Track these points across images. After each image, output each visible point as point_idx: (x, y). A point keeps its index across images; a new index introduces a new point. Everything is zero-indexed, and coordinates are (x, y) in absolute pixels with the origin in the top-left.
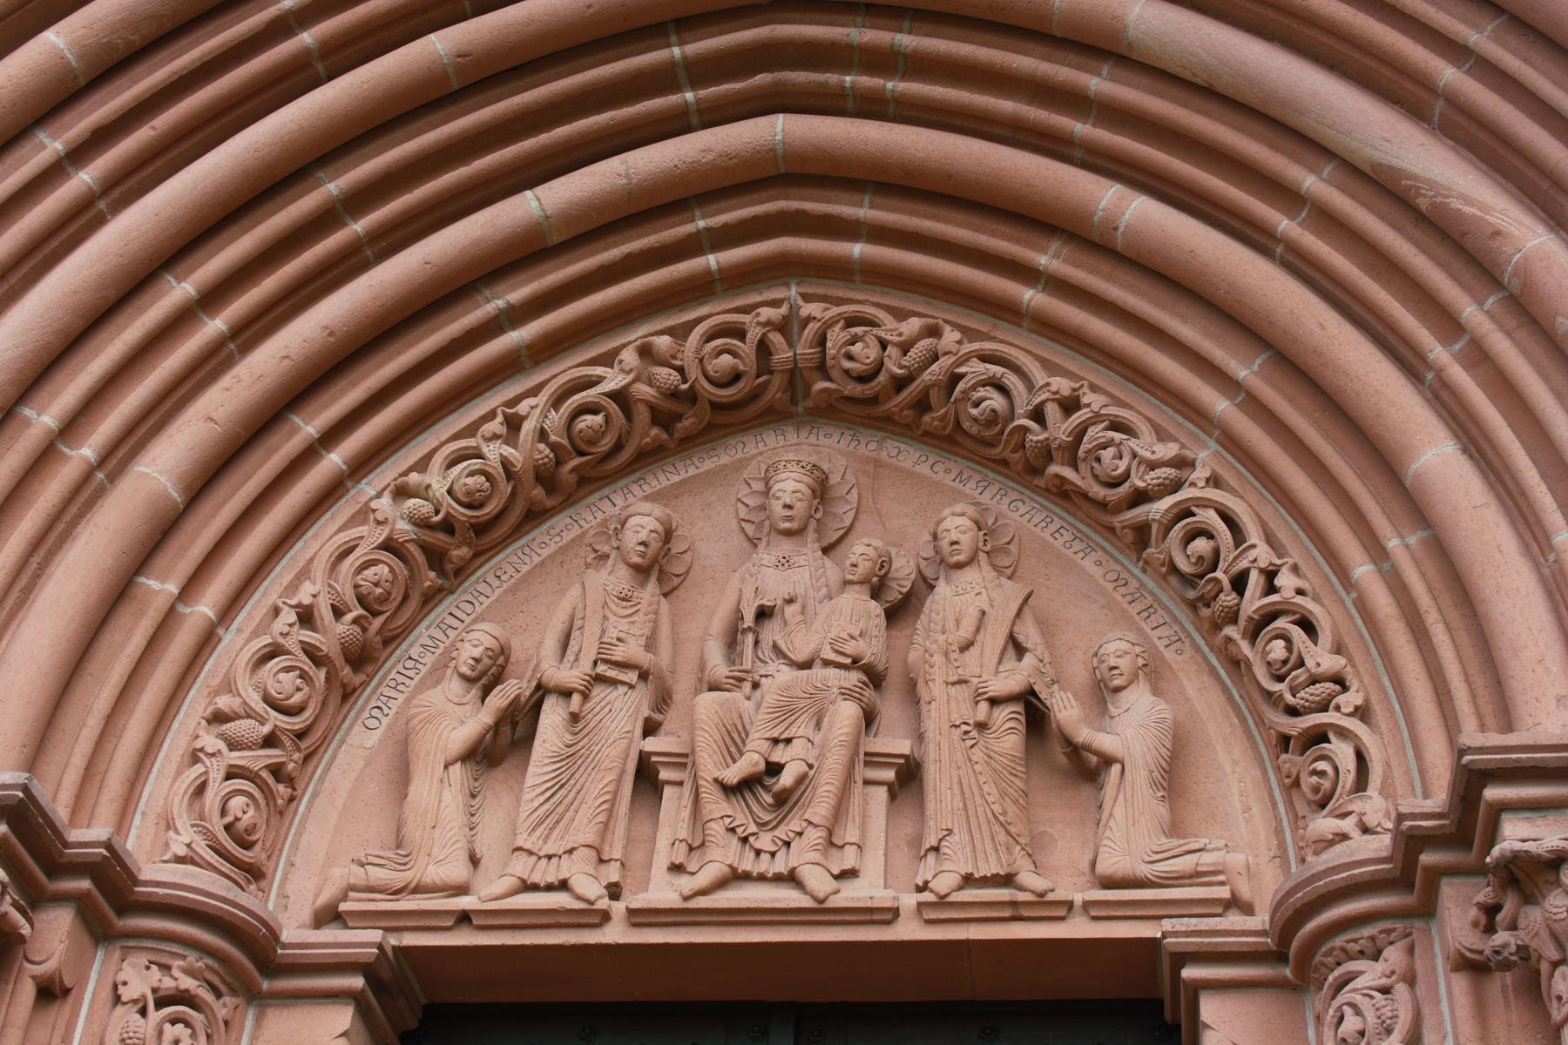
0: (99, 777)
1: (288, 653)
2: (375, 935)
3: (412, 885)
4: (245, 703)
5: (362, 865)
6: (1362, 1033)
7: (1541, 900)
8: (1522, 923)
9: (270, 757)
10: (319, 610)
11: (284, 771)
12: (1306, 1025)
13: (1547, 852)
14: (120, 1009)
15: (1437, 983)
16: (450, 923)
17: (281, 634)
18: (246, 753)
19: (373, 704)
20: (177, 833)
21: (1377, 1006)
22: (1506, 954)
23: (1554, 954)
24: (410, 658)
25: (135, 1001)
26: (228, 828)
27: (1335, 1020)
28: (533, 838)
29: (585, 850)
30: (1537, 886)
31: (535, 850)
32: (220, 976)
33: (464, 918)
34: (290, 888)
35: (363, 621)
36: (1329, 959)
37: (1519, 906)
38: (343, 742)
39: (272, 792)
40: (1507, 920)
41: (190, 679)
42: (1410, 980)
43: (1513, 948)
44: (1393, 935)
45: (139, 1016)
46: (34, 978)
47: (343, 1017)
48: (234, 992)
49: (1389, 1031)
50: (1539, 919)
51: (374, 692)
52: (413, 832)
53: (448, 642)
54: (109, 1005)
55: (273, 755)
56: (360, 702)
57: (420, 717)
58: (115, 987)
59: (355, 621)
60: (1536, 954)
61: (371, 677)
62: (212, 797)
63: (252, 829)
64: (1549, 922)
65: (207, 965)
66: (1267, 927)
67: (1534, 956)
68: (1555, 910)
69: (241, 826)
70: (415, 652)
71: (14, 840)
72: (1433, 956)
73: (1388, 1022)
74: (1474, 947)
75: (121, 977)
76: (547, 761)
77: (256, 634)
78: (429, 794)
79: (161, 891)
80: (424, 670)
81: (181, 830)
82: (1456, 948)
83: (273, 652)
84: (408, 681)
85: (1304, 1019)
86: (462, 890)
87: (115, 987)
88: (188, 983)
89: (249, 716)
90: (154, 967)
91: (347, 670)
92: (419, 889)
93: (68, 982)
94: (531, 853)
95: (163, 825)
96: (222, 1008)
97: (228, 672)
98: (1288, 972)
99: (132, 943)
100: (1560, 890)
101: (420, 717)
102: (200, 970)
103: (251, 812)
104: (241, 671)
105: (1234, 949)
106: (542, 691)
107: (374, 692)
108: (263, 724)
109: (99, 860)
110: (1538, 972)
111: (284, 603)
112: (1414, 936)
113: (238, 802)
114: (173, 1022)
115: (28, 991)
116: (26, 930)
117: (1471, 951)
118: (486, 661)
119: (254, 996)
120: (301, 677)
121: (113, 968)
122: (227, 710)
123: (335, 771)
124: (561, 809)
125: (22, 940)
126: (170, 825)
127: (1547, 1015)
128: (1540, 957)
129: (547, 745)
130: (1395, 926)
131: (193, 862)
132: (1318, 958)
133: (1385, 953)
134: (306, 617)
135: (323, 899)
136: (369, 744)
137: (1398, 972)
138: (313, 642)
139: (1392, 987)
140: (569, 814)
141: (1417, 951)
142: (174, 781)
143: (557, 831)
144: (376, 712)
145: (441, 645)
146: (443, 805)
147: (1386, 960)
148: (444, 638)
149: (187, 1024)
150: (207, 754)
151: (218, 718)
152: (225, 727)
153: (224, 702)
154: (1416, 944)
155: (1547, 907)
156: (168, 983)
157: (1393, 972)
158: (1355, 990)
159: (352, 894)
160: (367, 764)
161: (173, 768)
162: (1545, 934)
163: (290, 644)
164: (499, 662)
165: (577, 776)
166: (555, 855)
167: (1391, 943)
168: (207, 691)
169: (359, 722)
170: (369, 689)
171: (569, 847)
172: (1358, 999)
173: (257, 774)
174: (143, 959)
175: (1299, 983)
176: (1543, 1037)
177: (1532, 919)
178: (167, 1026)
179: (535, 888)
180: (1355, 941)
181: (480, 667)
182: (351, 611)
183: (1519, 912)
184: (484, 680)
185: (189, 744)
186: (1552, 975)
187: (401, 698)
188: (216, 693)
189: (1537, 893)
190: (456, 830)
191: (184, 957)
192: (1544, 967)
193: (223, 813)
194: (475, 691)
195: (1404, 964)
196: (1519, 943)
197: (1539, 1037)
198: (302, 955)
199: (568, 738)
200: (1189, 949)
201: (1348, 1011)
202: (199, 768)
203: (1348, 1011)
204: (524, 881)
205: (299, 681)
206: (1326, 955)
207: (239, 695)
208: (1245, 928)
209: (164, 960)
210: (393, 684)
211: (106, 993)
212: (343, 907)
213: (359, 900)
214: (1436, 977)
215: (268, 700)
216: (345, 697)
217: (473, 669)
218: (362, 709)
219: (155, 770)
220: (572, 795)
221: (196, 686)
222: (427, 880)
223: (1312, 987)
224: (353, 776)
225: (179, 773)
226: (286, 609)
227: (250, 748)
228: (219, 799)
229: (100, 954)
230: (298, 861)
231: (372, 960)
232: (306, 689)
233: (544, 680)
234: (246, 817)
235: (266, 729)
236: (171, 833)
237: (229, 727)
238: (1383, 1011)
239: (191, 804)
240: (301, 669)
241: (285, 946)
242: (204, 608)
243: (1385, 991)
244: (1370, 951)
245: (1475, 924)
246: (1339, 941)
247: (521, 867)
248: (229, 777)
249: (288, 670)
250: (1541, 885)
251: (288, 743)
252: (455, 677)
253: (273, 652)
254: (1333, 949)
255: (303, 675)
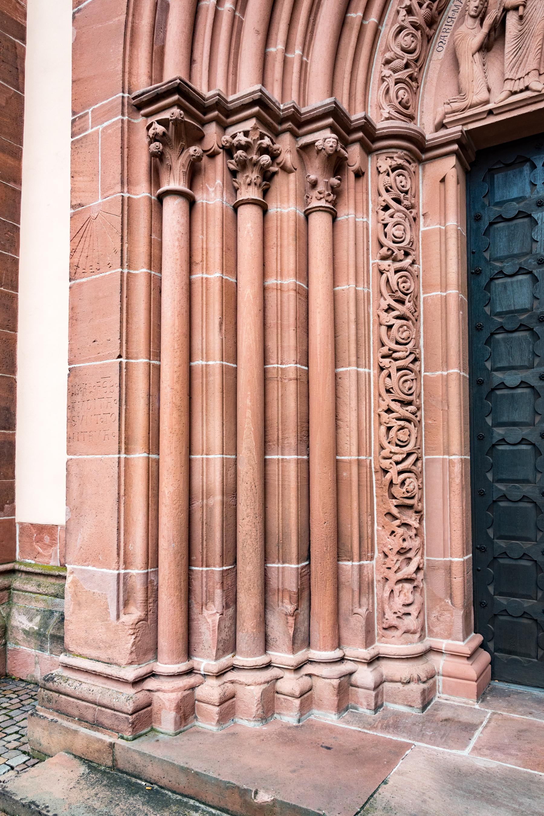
0: (354, 96)
1: (406, 28)
2: (459, 128)
3: (469, 106)
4: (395, 53)
5: (449, 104)
9: (408, 72)
10: (414, 6)
11: (413, 77)
14: (381, 175)
16: (485, 116)
17: (402, 21)
18: (400, 73)
19: (439, 41)
20: (384, 109)
24: (449, 17)
25: (385, 172)
26: (400, 103)
28: (512, 73)
29: (534, 71)
31: (513, 78)
32: (409, 157)
33: (490, 112)
34: (424, 121)
35: (430, 6)
38: (430, 60)
39: (411, 86)
41: (374, 50)
45: (387, 177)
46: (352, 171)
47: (452, 160)
48: (414, 161)
51: (438, 36)
52: (465, 85)
53: (462, 5)
54: (377, 175)
55: (409, 71)
56: (434, 42)
57: (459, 39)
58: (377, 169)
59: (428, 7)
61: (436, 30)
62: (392, 93)
63: (407, 102)
65: (405, 154)
69: (404, 101)
70: (450, 15)
71: (336, 124)
75: (378, 165)
76: (513, 40)
77: (393, 24)
78: (468, 69)
79: (385, 131)
80: (455, 20)
81: (385, 108)
83: (401, 29)
84: (450, 27)
86: (487, 102)
87: (377, 169)
88: (400, 161)
89: (398, 58)
90: (388, 159)
91: (428, 29)
92: (471, 107)
93: (363, 170)
94: (512, 79)
95: (378, 108)
96: (412, 167)
97: (386, 43)
99: (379, 152)
101: (459, 39)
102: (403, 156)
103: (406, 95)
104: (391, 41)
106: (506, 10)
107: (438, 36)
108: (403, 60)
109: (363, 124)
111: (400, 8)
113: (401, 92)
114: (399, 176)
115: (352, 176)
116: (347, 155)
118: (481, 6)
119: (420, 161)
120: (412, 37)
121: (375, 162)
122: (389, 58)
123: (430, 72)
124: (521, 58)
125: (346, 159)
126: (381, 108)
129: (512, 33)
131: (392, 119)
134: (409, 11)
135: (437, 121)
136: (440, 58)
138: (414, 20)
140: (525, 60)
142: (378, 91)
143: (521, 67)
144: (441, 44)
145: (460, 8)
146: (475, 71)
148: (460, 4)
149: (403, 175)
150: (387, 77)
151: (388, 62)
152: (390, 65)
153: (388, 55)
156: (394, 163)
159: (447, 116)
160: (441, 66)
161: (376, 86)
163: (406, 24)
164: (485, 6)
165: (525, 42)
166: (521, 78)
168: (381, 53)
169: (435, 50)
170: (436, 36)
171: (527, 72)
173: (405, 80)
174: (384, 157)
178: (397, 177)
179: (516, 93)
181: (478, 10)
182: (425, 3)
184: (480, 16)
185: (380, 75)
187: (449, 35)
188: (384, 52)
190: (481, 80)
191: (397, 153)
193: (397, 98)
194: (478, 22)
198: (434, 142)
199: (520, 27)
202: (385, 83)
204: (511, 91)
205: (412, 38)
207: (392, 51)
209: (391, 155)
210: (444, 30)
211: (375, 171)
212: (445, 121)
213: (450, 117)
215: (403, 50)
216: (429, 41)
217: (476, 11)
218: (435, 45)
219: (370, 89)
220: (525, 50)
221: (377, 52)
222: (474, 102)
224: (437, 72)
225: (379, 87)
226: (401, 10)
227: (401, 70)
228: (395, 93)
229: (370, 159)
230: (424, 110)
231: (460, 137)
232: (415, 41)
233: (506, 6)
234: (405, 97)
235: (405, 61)
236: (382, 110)
237: (392, 65)
239: (385, 98)
240: (412, 33)
241: (428, 141)
242: (373, 19)
247: (509, 86)
248: (396, 84)
249: (407, 35)
251: (413, 65)
252: (469, 18)
253: (401, 29)
255: (413, 36)
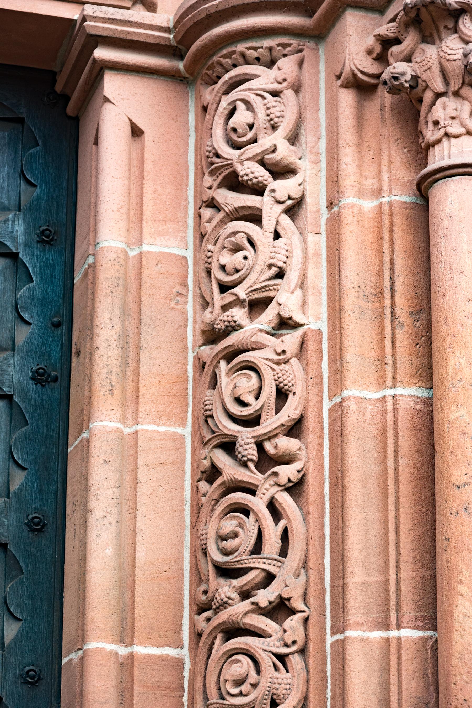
6: (251, 127)
7: (437, 41)
8: (417, 57)
12: (188, 111)
13: (456, 2)
15: (318, 94)
21: (268, 105)
22: (402, 80)
23: (440, 87)
27: (226, 112)
30: (438, 30)
36: (227, 60)
37: (417, 43)
40: (405, 53)
42: (297, 89)
43: (408, 77)
44: (288, 49)
49: (274, 128)
50: (435, 56)
60: (424, 84)
64: (443, 60)
66: (171, 25)
67: (421, 85)
68: (450, 52)
72: (318, 72)
73: (276, 120)
74: (365, 70)
82: (351, 69)
85: (187, 106)
98: (181, 65)
100: (456, 35)
105: (142, 39)
110: (420, 100)
112: (304, 53)
117: (362, 72)
127: (418, 134)
128: (427, 86)
130: (291, 42)
132: (216, 58)
133: (281, 62)
137: (289, 80)
139: (281, 92)
141: (305, 65)
147: (280, 69)
154: (306, 60)
155: (444, 48)
157: (285, 80)
158: (250, 89)
162: (436, 70)
167: (285, 55)
172: (252, 98)
175: (187, 75)
176: (409, 151)
177: (428, 55)
180: (255, 49)
183: (417, 47)
186: (433, 104)
189: (435, 35)
192: (428, 96)
195: (294, 74)
196: (413, 73)
197: (406, 150)
200: (104, 34)
201: (241, 106)
203: (241, 106)
206: (225, 56)
208: (153, 23)
214: (318, 88)
223: (199, 81)
238: (272, 110)
243: (275, 94)
244: (266, 57)
245: (369, 52)
246: (240, 47)
250: (442, 29)
254: (234, 52)
